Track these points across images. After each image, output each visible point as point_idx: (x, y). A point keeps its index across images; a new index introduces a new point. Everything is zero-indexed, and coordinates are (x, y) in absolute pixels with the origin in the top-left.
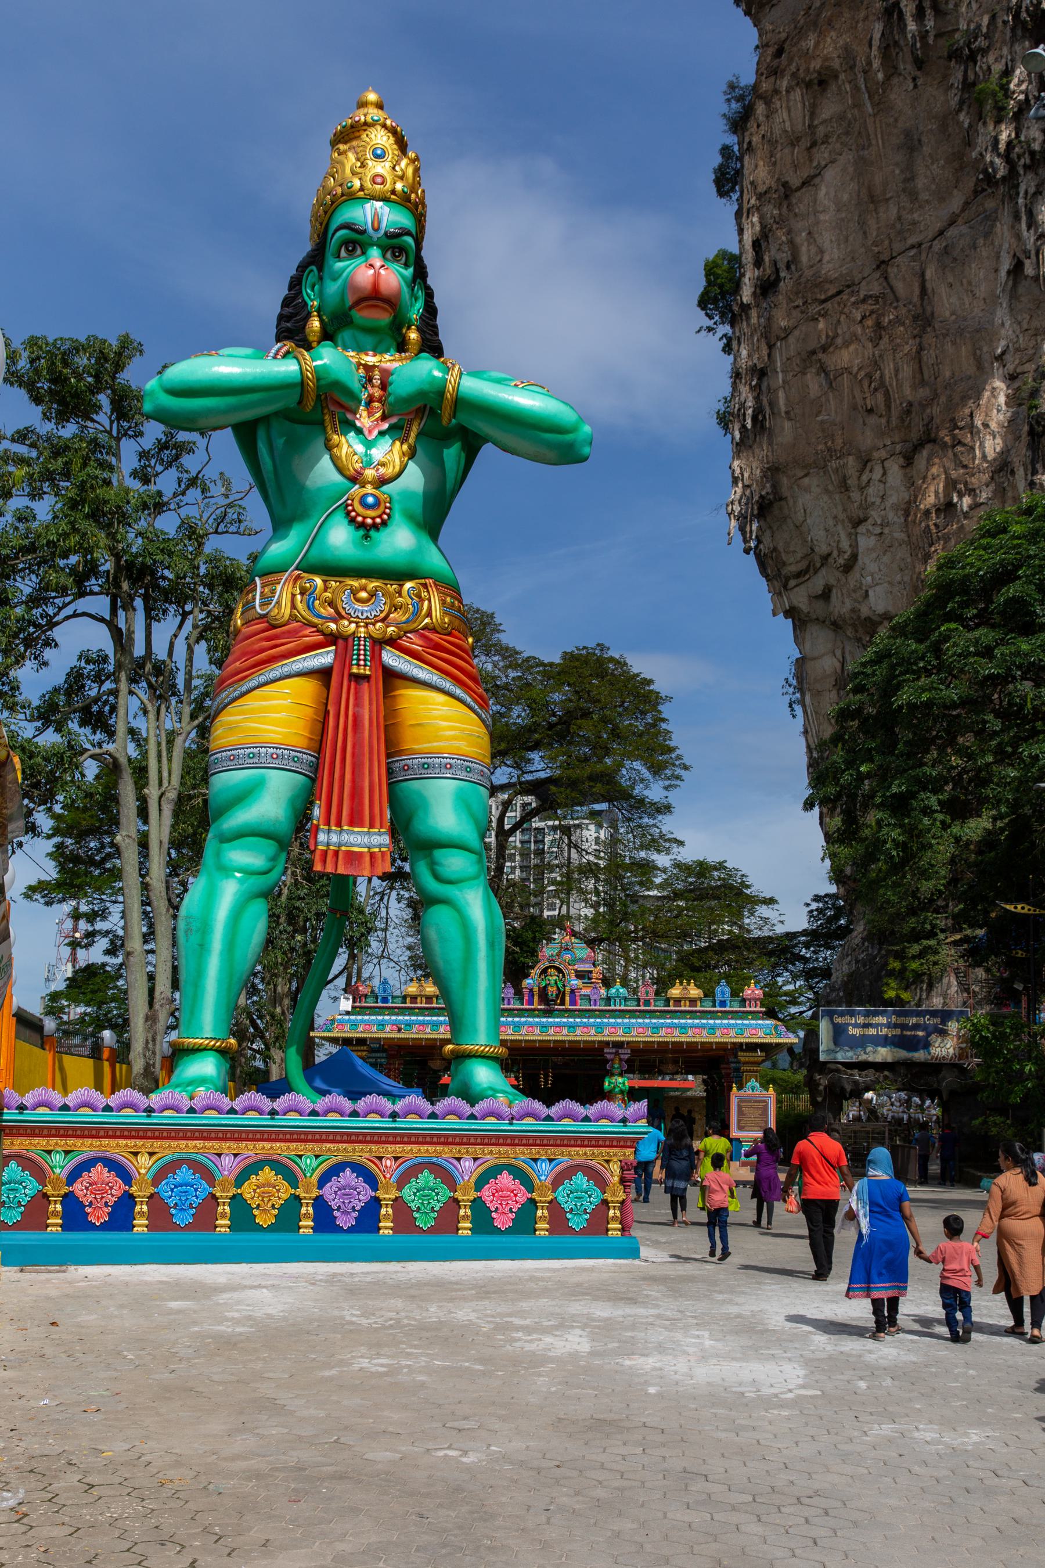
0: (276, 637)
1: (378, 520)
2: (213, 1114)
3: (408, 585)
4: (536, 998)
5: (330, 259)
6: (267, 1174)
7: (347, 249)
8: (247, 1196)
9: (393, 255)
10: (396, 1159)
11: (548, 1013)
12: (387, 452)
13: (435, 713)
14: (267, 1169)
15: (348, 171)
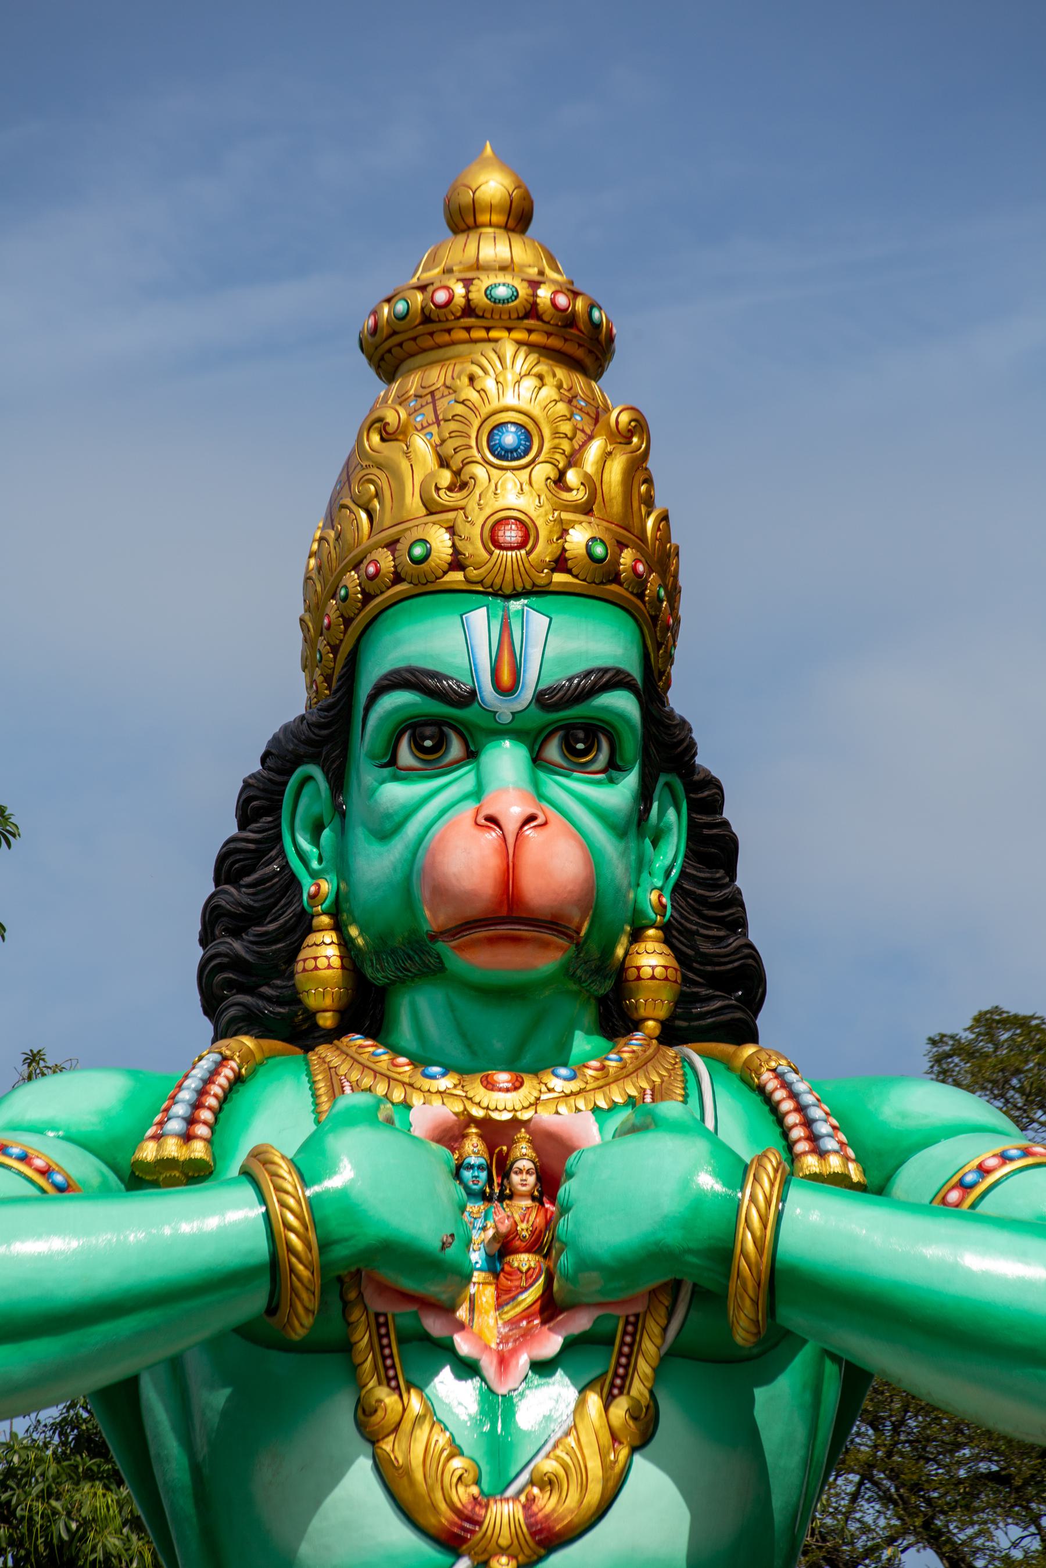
5: (365, 772)
7: (417, 746)
9: (569, 749)
15: (413, 503)
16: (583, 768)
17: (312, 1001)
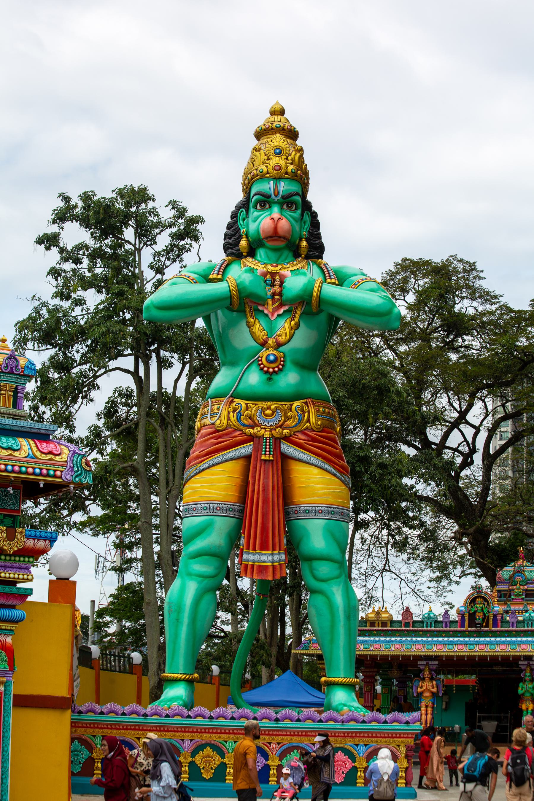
0: (220, 437)
1: (276, 369)
2: (179, 718)
3: (296, 404)
4: (467, 622)
5: (251, 210)
6: (208, 751)
7: (260, 205)
8: (198, 762)
9: (288, 206)
10: (279, 744)
11: (479, 634)
12: (283, 326)
13: (312, 480)
14: (208, 748)
16: (290, 210)
17: (242, 250)
